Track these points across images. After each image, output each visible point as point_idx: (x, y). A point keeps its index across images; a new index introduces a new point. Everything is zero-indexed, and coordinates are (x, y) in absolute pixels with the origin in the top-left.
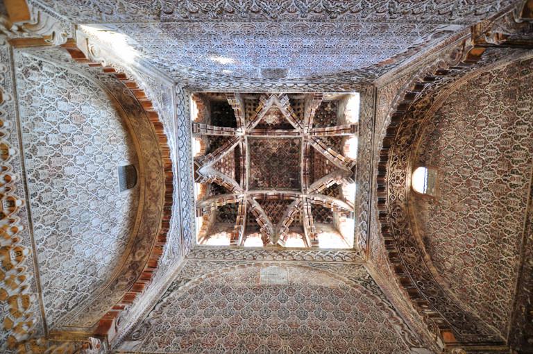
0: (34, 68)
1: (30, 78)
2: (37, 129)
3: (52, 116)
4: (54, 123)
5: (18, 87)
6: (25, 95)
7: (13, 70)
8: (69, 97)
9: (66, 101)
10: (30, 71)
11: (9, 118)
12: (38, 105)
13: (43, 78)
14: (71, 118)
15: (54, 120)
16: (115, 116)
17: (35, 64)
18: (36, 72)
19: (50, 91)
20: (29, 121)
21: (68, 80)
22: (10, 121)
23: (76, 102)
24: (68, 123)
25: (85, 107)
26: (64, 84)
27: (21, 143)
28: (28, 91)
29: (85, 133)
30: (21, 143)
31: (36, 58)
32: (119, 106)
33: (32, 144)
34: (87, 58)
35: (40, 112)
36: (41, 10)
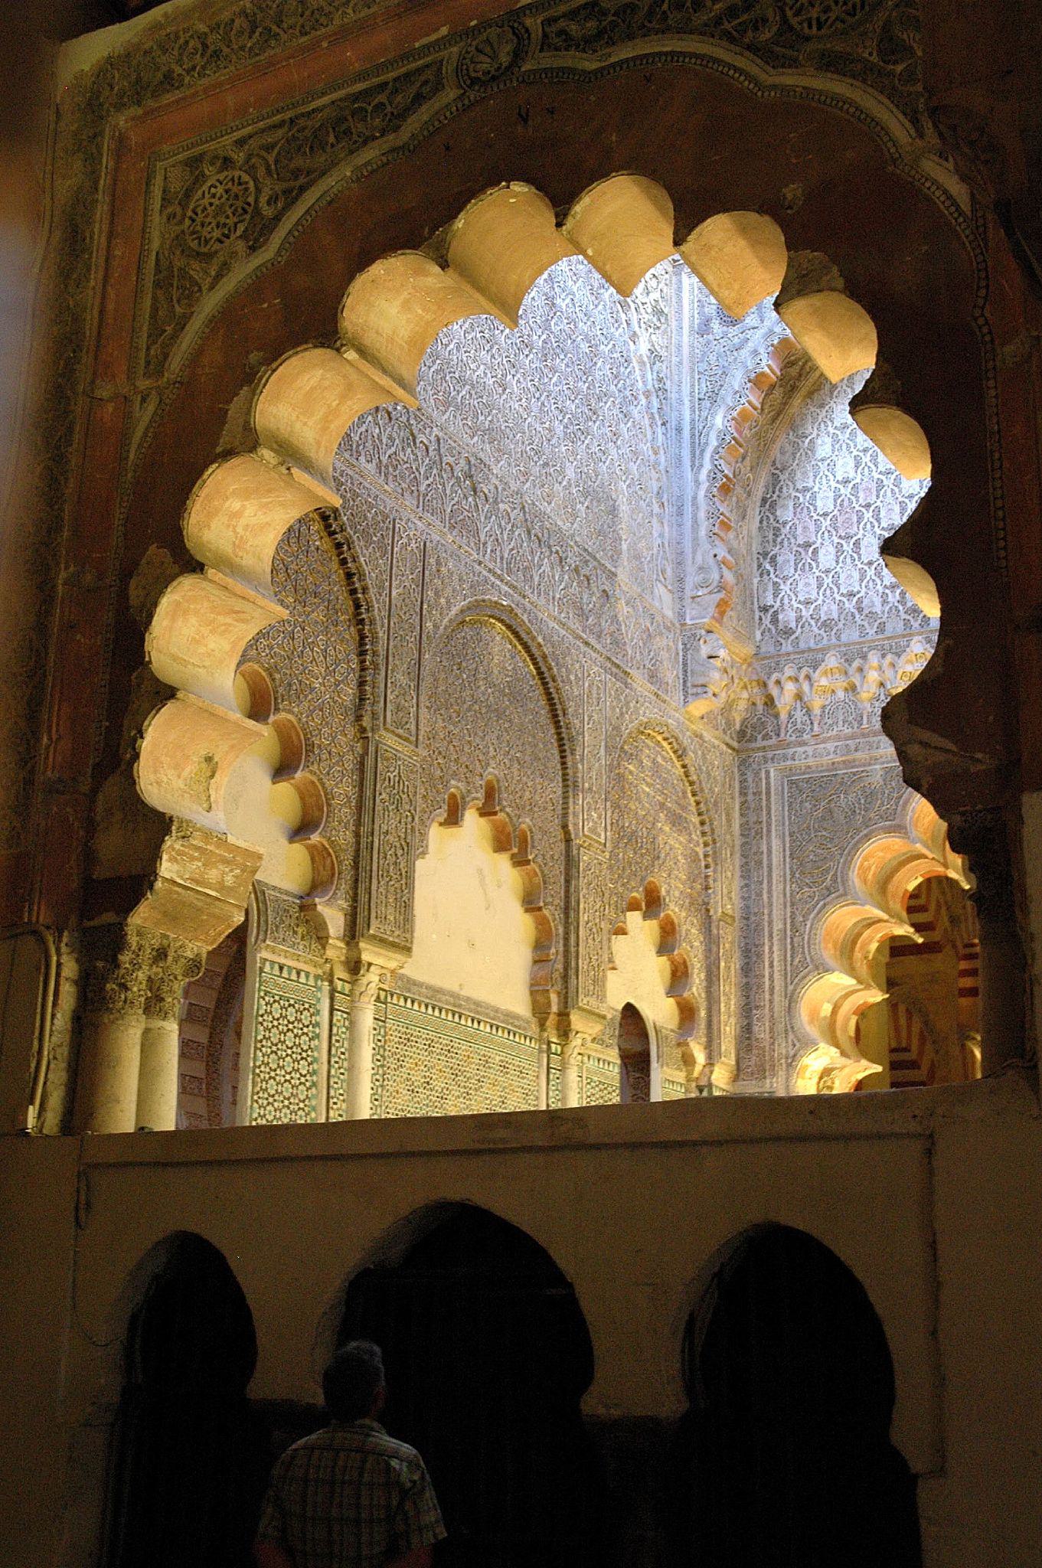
0: (775, 620)
1: (793, 625)
2: (878, 609)
3: (850, 578)
4: (863, 575)
5: (812, 645)
6: (822, 632)
7: (788, 654)
8: (807, 545)
9: (815, 552)
10: (781, 626)
11: (864, 657)
12: (834, 607)
13: (786, 601)
14: (848, 537)
15: (856, 575)
16: (822, 406)
17: (767, 620)
18: (780, 617)
19: (806, 586)
20: (865, 623)
21: (776, 550)
22: (870, 656)
23: (812, 528)
24: (857, 544)
25: (819, 503)
26: (786, 557)
27: (904, 636)
28: (815, 629)
29: (874, 498)
30: (904, 636)
31: (757, 617)
32: (797, 401)
33: (904, 616)
34: (722, 595)
35: (847, 605)
36: (689, 684)
